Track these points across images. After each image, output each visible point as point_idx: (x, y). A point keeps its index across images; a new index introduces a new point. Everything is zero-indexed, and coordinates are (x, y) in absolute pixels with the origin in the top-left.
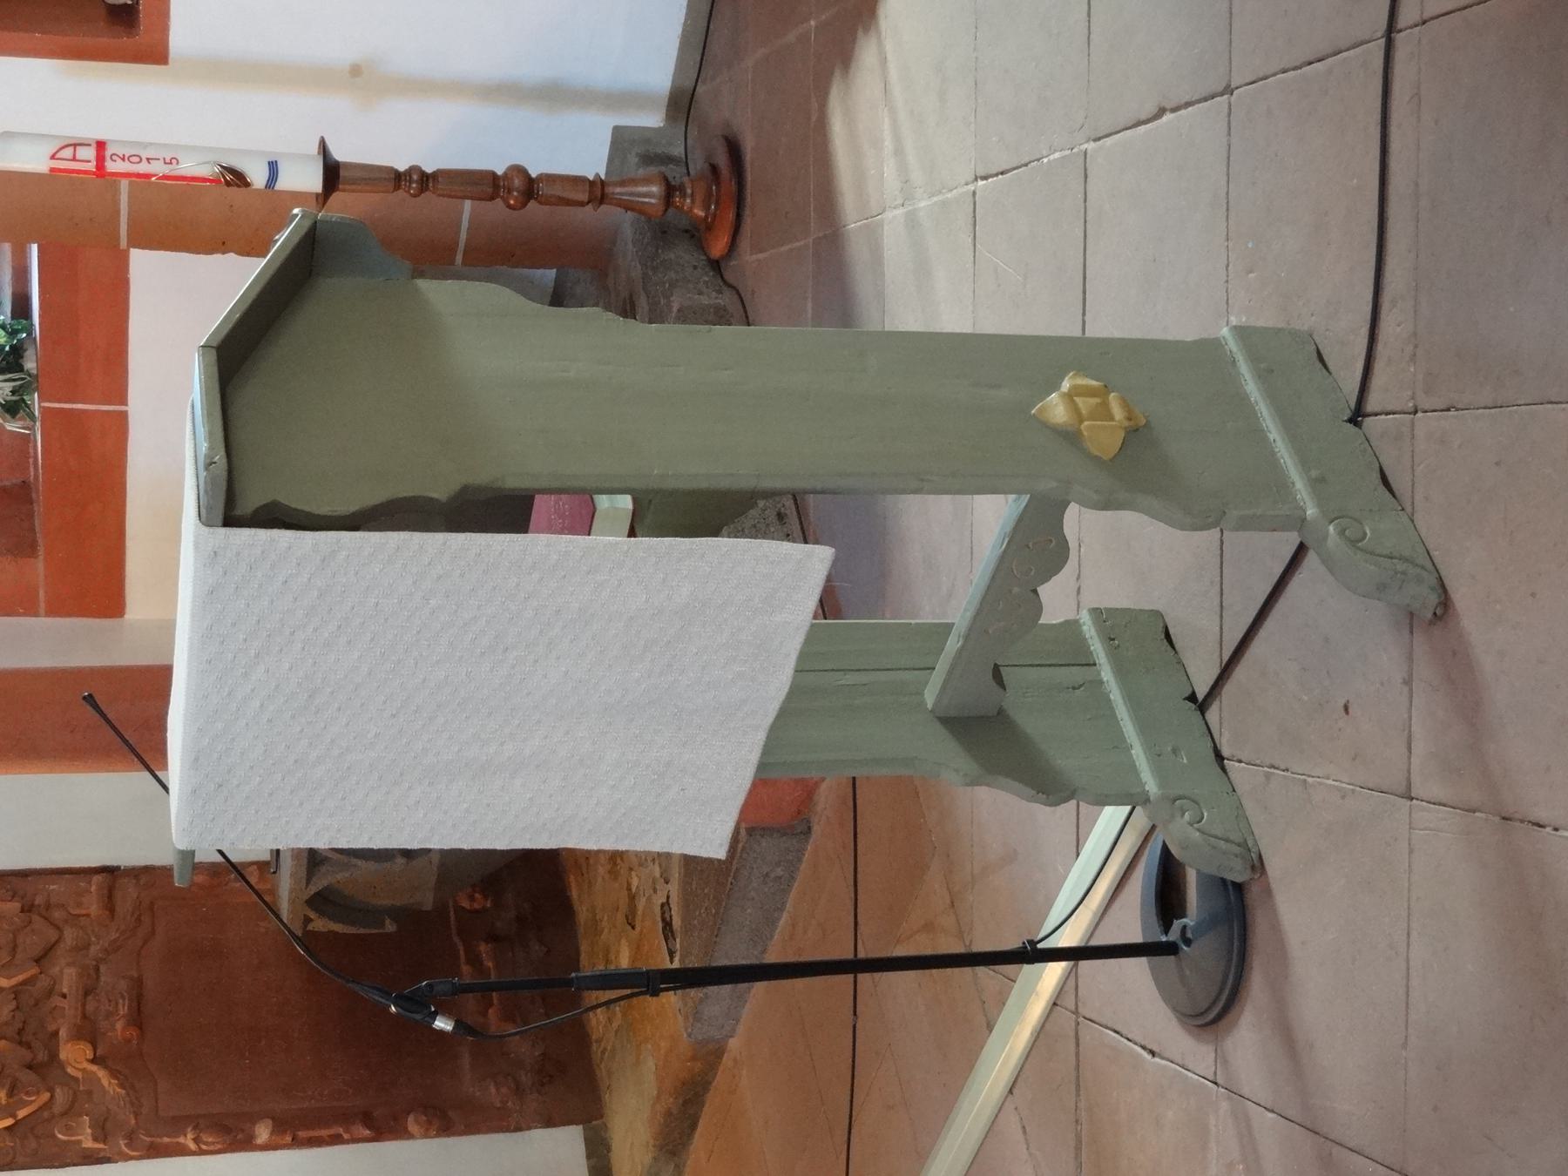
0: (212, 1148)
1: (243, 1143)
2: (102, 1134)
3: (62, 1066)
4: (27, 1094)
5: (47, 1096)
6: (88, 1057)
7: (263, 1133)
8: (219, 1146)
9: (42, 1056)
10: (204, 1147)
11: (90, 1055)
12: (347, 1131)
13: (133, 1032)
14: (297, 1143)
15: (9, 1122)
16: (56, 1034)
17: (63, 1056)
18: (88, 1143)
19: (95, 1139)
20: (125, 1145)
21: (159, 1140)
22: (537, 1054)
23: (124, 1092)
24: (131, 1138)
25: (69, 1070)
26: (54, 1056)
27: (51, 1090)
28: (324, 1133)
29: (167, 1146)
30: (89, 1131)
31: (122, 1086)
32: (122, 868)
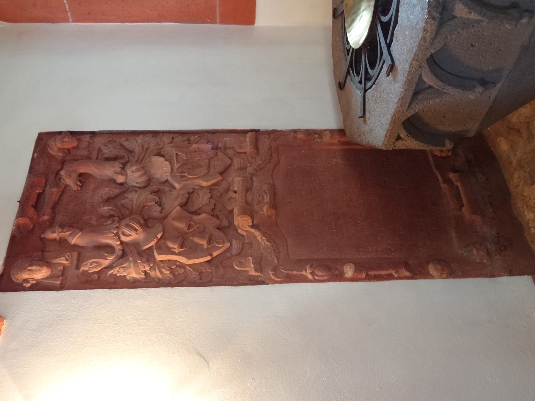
0: (321, 278)
1: (339, 277)
2: (259, 267)
3: (235, 229)
4: (218, 243)
5: (228, 244)
6: (249, 225)
7: (349, 271)
8: (325, 278)
9: (225, 223)
10: (317, 278)
11: (251, 224)
12: (397, 272)
13: (273, 212)
14: (369, 278)
15: (209, 258)
16: (231, 211)
17: (236, 223)
18: (253, 273)
19: (256, 270)
20: (272, 274)
21: (291, 272)
22: (494, 233)
23: (270, 244)
24: (275, 270)
25: (240, 231)
26: (231, 224)
27: (231, 242)
28: (383, 273)
29: (296, 276)
30: (252, 265)
31: (268, 241)
32: (261, 130)
